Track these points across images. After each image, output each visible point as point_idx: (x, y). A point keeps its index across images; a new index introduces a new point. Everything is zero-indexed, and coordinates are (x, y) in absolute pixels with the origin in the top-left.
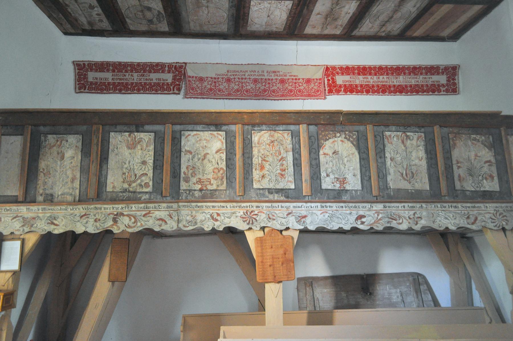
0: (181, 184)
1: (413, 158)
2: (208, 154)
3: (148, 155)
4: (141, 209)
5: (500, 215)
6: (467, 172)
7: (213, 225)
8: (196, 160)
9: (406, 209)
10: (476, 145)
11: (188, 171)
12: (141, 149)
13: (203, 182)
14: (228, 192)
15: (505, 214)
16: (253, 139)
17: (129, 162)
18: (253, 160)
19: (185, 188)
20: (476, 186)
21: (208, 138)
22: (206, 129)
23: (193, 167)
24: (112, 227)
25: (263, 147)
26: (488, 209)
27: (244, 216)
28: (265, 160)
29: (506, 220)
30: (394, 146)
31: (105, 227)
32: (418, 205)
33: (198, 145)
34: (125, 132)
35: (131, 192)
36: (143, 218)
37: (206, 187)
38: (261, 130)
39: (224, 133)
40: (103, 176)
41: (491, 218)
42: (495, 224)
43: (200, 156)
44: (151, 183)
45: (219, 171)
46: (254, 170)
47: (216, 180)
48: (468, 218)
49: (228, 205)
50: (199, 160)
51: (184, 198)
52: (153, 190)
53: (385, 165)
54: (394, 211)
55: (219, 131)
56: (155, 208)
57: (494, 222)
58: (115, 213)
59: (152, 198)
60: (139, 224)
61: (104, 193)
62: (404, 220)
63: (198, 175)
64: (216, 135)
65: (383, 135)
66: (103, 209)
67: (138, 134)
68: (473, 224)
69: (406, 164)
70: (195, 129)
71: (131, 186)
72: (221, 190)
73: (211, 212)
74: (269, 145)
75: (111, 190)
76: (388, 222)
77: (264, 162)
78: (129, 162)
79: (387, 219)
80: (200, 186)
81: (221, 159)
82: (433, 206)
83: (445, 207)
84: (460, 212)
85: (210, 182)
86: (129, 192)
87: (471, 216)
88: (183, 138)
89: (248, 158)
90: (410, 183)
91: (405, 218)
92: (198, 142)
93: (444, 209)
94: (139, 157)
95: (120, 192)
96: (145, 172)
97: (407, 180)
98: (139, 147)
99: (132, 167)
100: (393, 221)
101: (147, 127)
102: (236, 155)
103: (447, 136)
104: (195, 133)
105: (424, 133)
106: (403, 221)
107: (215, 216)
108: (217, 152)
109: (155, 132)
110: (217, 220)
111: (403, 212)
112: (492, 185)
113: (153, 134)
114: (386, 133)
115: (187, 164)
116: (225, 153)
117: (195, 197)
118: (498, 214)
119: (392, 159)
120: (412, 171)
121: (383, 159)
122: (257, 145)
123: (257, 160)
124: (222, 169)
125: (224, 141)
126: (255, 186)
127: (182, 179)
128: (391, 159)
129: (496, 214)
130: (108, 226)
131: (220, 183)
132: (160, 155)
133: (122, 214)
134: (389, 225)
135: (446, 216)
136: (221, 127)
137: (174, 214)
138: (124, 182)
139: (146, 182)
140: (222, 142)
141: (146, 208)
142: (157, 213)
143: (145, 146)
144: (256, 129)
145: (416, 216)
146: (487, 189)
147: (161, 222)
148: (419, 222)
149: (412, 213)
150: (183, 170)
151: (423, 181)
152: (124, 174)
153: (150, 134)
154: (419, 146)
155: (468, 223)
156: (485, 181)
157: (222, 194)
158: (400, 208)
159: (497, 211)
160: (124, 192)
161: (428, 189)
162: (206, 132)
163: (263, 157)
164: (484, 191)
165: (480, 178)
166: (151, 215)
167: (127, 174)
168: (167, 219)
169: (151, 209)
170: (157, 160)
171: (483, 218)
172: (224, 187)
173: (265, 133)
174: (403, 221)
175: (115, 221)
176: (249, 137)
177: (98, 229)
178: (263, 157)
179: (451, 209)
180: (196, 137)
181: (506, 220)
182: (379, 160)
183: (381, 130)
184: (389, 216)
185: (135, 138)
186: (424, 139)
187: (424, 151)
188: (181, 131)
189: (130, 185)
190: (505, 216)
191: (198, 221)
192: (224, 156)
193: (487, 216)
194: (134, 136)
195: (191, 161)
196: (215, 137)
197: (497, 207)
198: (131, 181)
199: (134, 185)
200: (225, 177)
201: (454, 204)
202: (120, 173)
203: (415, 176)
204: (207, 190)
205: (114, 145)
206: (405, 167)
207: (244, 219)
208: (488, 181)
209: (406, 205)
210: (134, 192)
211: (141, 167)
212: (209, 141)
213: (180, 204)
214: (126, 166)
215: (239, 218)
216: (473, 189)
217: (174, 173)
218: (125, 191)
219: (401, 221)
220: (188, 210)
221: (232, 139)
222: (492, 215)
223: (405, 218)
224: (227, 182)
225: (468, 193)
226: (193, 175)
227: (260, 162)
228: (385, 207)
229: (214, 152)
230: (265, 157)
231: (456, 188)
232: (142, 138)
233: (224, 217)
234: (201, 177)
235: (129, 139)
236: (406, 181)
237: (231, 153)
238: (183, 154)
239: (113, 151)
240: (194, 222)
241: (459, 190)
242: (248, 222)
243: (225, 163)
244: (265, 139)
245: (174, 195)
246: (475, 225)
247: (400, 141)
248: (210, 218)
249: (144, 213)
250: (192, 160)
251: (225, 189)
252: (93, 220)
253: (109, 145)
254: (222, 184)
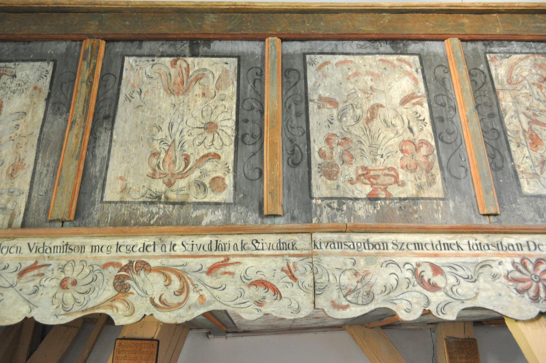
0: (313, 182)
2: (381, 106)
3: (221, 109)
4: (202, 252)
7: (423, 302)
8: (349, 120)
11: (332, 148)
12: (204, 94)
13: (376, 177)
16: (493, 73)
17: (171, 126)
18: (506, 120)
19: (326, 193)
21: (376, 71)
22: (368, 50)
23: (345, 139)
24: (112, 307)
25: (525, 91)
27: (517, 275)
28: (537, 123)
31: (90, 305)
33: (351, 86)
34: (162, 56)
35: (174, 204)
36: (208, 280)
37: (385, 189)
38: (511, 53)
39: (417, 58)
40: (98, 161)
43: (358, 112)
44: (229, 180)
45: (417, 149)
46: (513, 147)
47: (413, 171)
49: (464, 240)
50: (358, 120)
51: (325, 220)
52: (234, 198)
55: (402, 54)
56: (243, 248)
58: (124, 262)
59: (233, 220)
60: (194, 297)
61: (98, 206)
63: (359, 158)
64: (396, 62)
66: (88, 249)
67: (197, 60)
70: (340, 49)
71: (174, 187)
72: (430, 199)
73: (414, 261)
75: (117, 198)
78: (171, 126)
80: (368, 189)
81: (417, 116)
85: (396, 177)
86: (168, 202)
88: (311, 71)
89: (491, 116)
92: (352, 80)
94: (197, 113)
95: (140, 203)
96: (212, 150)
98: (197, 89)
99: (178, 138)
101: (217, 46)
102: (455, 109)
104: (341, 58)
107: (428, 274)
108: (404, 101)
109: (239, 57)
110: (434, 287)
113: (235, 60)
115: (325, 132)
116: (426, 105)
117: (357, 218)
122: (507, 86)
123: (515, 121)
124: (423, 142)
125: (420, 77)
126: (528, 187)
127: (314, 169)
130: (99, 301)
131: (424, 180)
132: (252, 108)
133: (144, 266)
136: (405, 46)
137: (302, 265)
138: (153, 176)
139: (214, 175)
140: (415, 79)
141: (217, 248)
142: (249, 262)
143: (212, 87)
144: (495, 49)
147: (261, 291)
150: (315, 147)
152: (155, 154)
153: (225, 60)
157: (437, 211)
160: (152, 203)
162: (370, 57)
163: (530, 113)
166: (230, 269)
167: (163, 155)
168: (280, 281)
169: (232, 252)
170: (246, 121)
172: (437, 190)
173: (521, 60)
175: (121, 286)
176: (482, 67)
177: (68, 312)
178: (530, 113)
180: (345, 67)
185: (188, 70)
188: (304, 55)
189: (170, 184)
191: (377, 289)
192: (424, 111)
194: (184, 65)
195: (336, 123)
196: (394, 66)
198: (173, 175)
199: (181, 183)
200: (437, 164)
202: (146, 152)
204: (389, 197)
205: (133, 86)
207: (521, 286)
210: (182, 204)
211: (201, 139)
212: (378, 76)
213: (318, 237)
214: (160, 135)
215: (503, 280)
217: (293, 151)
218: (156, 199)
220: (343, 254)
221: (439, 72)
224: (444, 179)
226: (346, 158)
227: (526, 127)
229: (397, 100)
230: (535, 114)
232: (205, 70)
233: (456, 276)
234: (367, 163)
235: (173, 71)
237: (443, 105)
238: (312, 106)
239: (129, 98)
240: (363, 292)
242: (532, 293)
243: (429, 128)
244: (525, 73)
245: (296, 212)
248: (413, 280)
249: (209, 262)
250: (340, 120)
251: (441, 195)
252: (55, 283)
253: (120, 84)
254: (431, 183)
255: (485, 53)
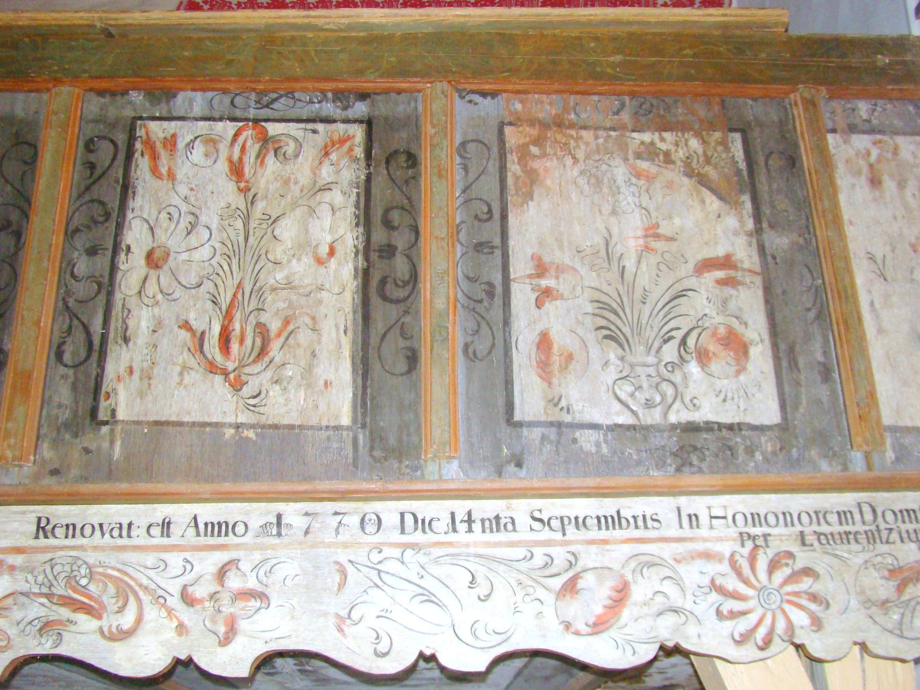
1: (278, 253)
5: (773, 566)
6: (588, 320)
9: (174, 540)
10: (651, 179)
15: (803, 559)
20: (641, 396)
26: (704, 532)
29: (814, 598)
30: (183, 190)
32: (257, 514)
41: (721, 590)
42: (743, 625)
48: (571, 588)
53: (110, 294)
54: (91, 558)
57: (733, 615)
62: (152, 614)
65: (132, 138)
68: (599, 626)
69: (231, 284)
76: (46, 627)
79: (37, 610)
82: (355, 520)
83: (425, 525)
84: (521, 552)
87: (587, 581)
90: (237, 385)
91: (160, 600)
93: (418, 537)
97: (225, 373)
100: (81, 617)
103: (491, 138)
105: (369, 123)
106: (139, 620)
111: (150, 559)
112: (747, 394)
114: (153, 125)
118: (762, 564)
119: (154, 260)
120: (264, 318)
121: (102, 262)
128: (149, 255)
129: (752, 560)
134: (46, 648)
135: (429, 583)
145: (234, 582)
146: (707, 412)
148: (243, 625)
149: (210, 563)
151: (323, 371)
154: (326, 188)
155: (567, 626)
156: (693, 368)
158: (139, 537)
159: (757, 544)
161: (346, 420)
164: (691, 428)
165: (670, 352)
171: (668, 587)
174: (139, 620)
179: (462, 535)
181: (814, 598)
182: (82, 266)
183: (128, 113)
184: (60, 590)
186: (359, 152)
187: (350, 211)
190: (807, 572)
193: (695, 574)
197: (756, 519)
201: (485, 508)
203: (275, 346)
206: (225, 299)
208: (715, 367)
209: (180, 512)
216: (624, 419)
219: (127, 620)
222: (725, 567)
223: (160, 600)
225: (588, 440)
228: (42, 529)
231: (517, 417)
236: (219, 379)
241: (531, 424)
246: (613, 632)
247: (222, 166)
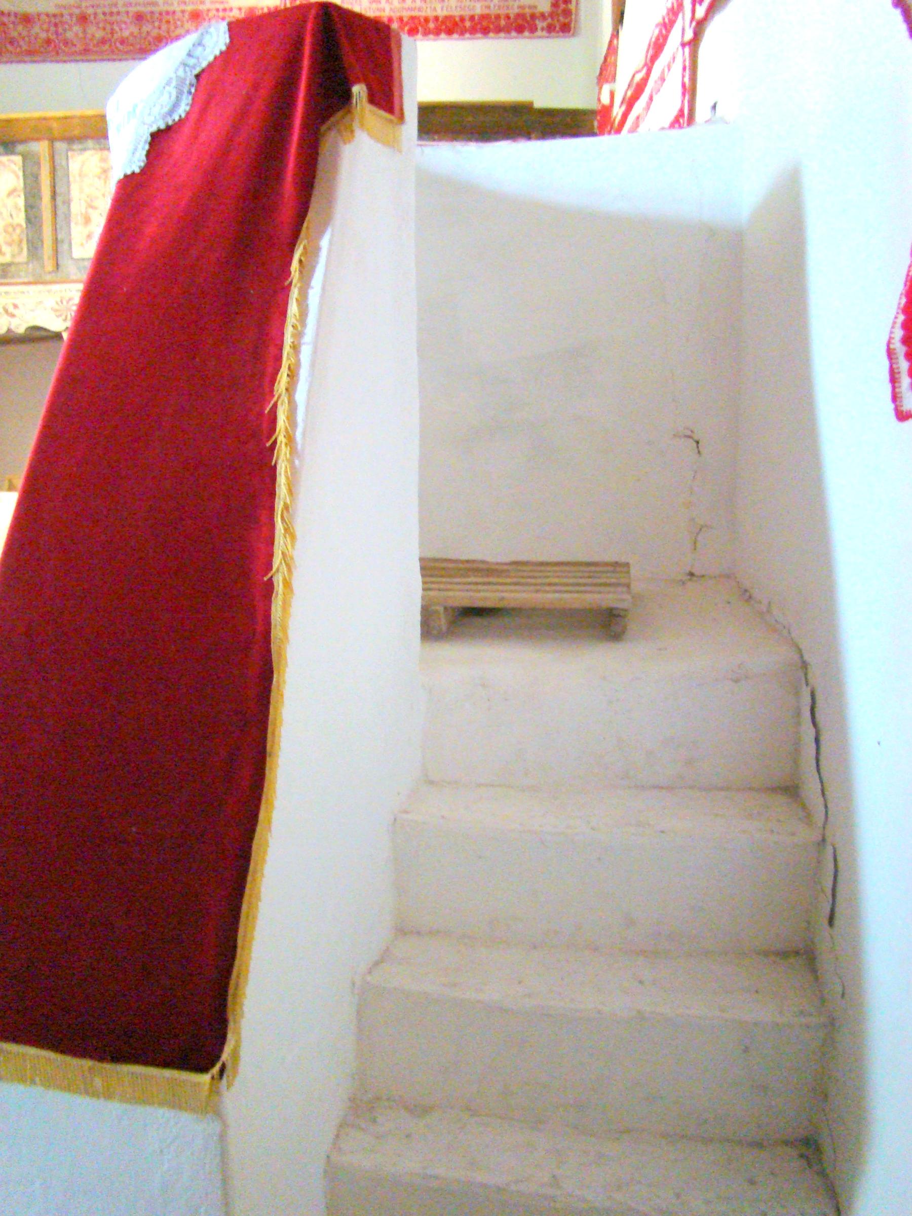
14: (31, 265)
38: (85, 150)
45: (14, 229)
64: (7, 163)
74: (99, 178)
77: (90, 210)
81: (16, 207)
107: (11, 309)
110: (13, 316)
124: (19, 225)
125: (21, 174)
172: (23, 257)
178: (89, 200)
192: (21, 202)
242: (63, 317)
255: (67, 151)
